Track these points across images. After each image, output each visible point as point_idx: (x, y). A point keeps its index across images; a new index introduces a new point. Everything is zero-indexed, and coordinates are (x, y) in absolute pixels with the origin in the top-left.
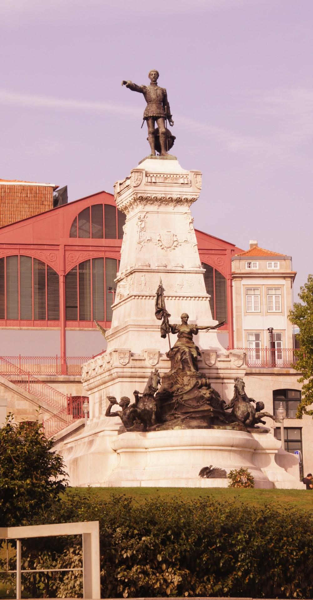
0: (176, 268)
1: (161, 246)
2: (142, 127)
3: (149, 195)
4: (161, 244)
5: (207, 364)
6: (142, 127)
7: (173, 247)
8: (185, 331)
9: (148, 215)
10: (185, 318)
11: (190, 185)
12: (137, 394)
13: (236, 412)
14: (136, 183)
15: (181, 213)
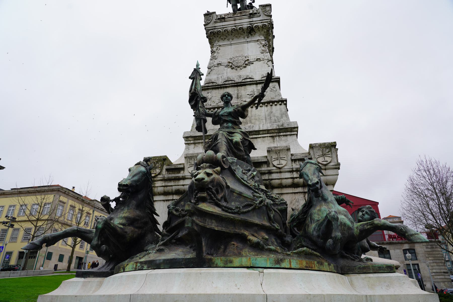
0: (245, 80)
1: (231, 66)
2: (227, 7)
3: (219, 30)
4: (231, 64)
5: (274, 166)
6: (227, 7)
7: (244, 65)
8: (225, 113)
9: (221, 48)
10: (227, 99)
11: (259, 14)
12: (105, 203)
13: (308, 226)
14: (206, 22)
15: (255, 41)
